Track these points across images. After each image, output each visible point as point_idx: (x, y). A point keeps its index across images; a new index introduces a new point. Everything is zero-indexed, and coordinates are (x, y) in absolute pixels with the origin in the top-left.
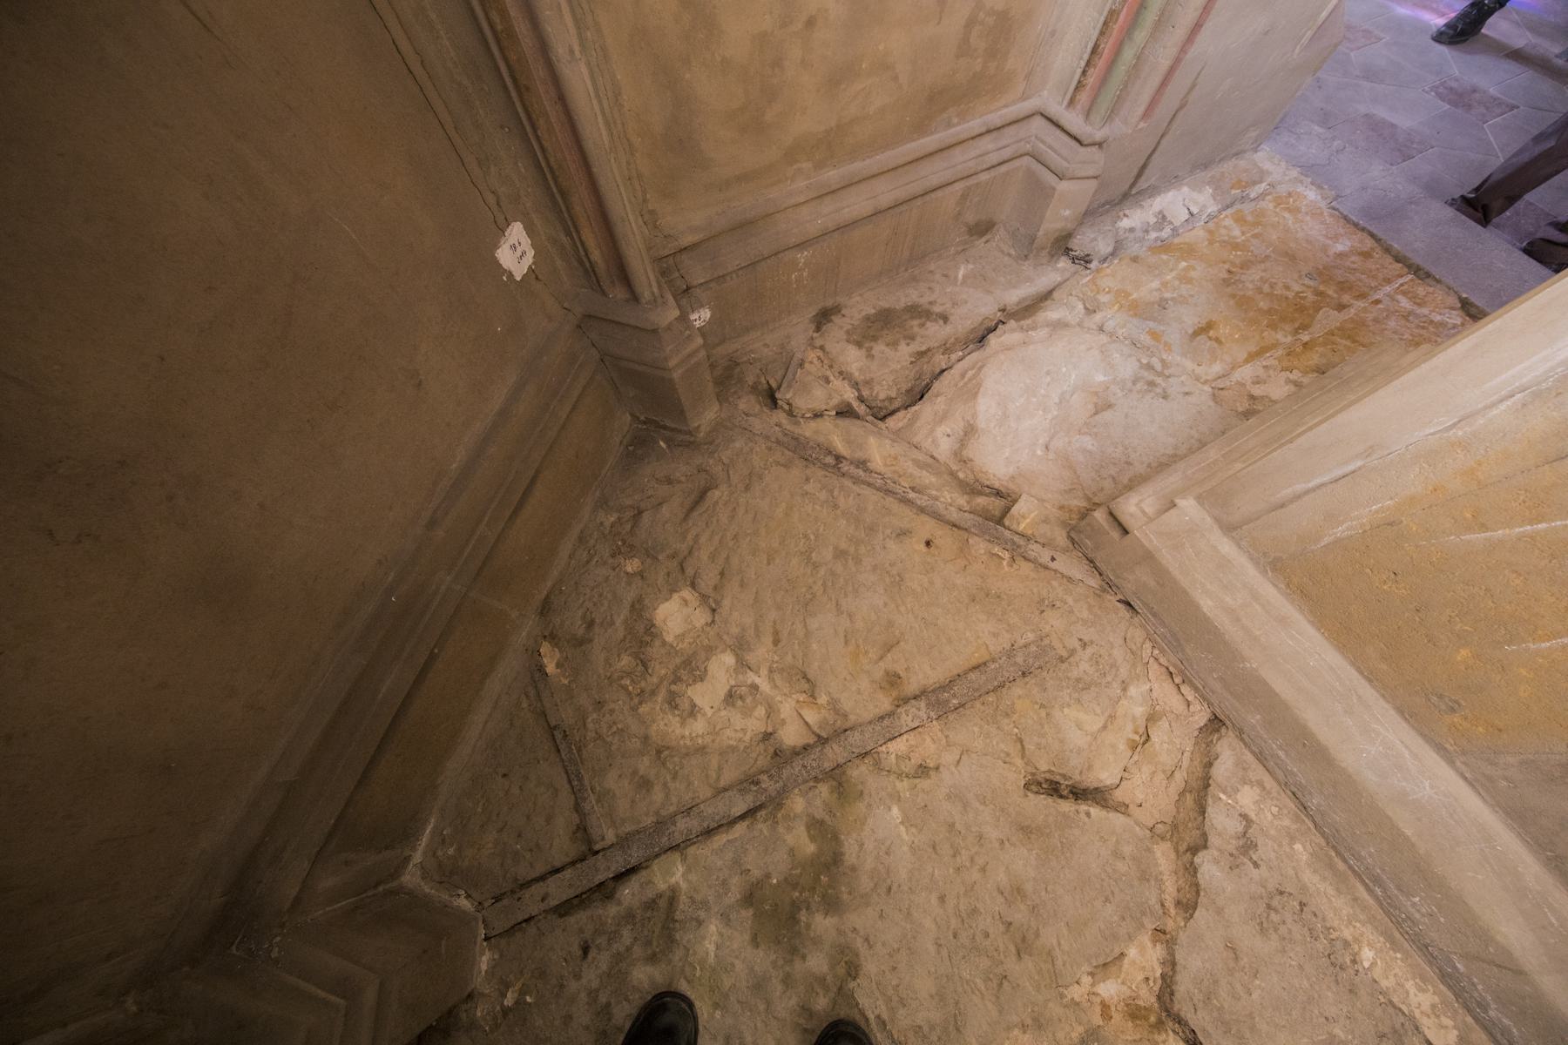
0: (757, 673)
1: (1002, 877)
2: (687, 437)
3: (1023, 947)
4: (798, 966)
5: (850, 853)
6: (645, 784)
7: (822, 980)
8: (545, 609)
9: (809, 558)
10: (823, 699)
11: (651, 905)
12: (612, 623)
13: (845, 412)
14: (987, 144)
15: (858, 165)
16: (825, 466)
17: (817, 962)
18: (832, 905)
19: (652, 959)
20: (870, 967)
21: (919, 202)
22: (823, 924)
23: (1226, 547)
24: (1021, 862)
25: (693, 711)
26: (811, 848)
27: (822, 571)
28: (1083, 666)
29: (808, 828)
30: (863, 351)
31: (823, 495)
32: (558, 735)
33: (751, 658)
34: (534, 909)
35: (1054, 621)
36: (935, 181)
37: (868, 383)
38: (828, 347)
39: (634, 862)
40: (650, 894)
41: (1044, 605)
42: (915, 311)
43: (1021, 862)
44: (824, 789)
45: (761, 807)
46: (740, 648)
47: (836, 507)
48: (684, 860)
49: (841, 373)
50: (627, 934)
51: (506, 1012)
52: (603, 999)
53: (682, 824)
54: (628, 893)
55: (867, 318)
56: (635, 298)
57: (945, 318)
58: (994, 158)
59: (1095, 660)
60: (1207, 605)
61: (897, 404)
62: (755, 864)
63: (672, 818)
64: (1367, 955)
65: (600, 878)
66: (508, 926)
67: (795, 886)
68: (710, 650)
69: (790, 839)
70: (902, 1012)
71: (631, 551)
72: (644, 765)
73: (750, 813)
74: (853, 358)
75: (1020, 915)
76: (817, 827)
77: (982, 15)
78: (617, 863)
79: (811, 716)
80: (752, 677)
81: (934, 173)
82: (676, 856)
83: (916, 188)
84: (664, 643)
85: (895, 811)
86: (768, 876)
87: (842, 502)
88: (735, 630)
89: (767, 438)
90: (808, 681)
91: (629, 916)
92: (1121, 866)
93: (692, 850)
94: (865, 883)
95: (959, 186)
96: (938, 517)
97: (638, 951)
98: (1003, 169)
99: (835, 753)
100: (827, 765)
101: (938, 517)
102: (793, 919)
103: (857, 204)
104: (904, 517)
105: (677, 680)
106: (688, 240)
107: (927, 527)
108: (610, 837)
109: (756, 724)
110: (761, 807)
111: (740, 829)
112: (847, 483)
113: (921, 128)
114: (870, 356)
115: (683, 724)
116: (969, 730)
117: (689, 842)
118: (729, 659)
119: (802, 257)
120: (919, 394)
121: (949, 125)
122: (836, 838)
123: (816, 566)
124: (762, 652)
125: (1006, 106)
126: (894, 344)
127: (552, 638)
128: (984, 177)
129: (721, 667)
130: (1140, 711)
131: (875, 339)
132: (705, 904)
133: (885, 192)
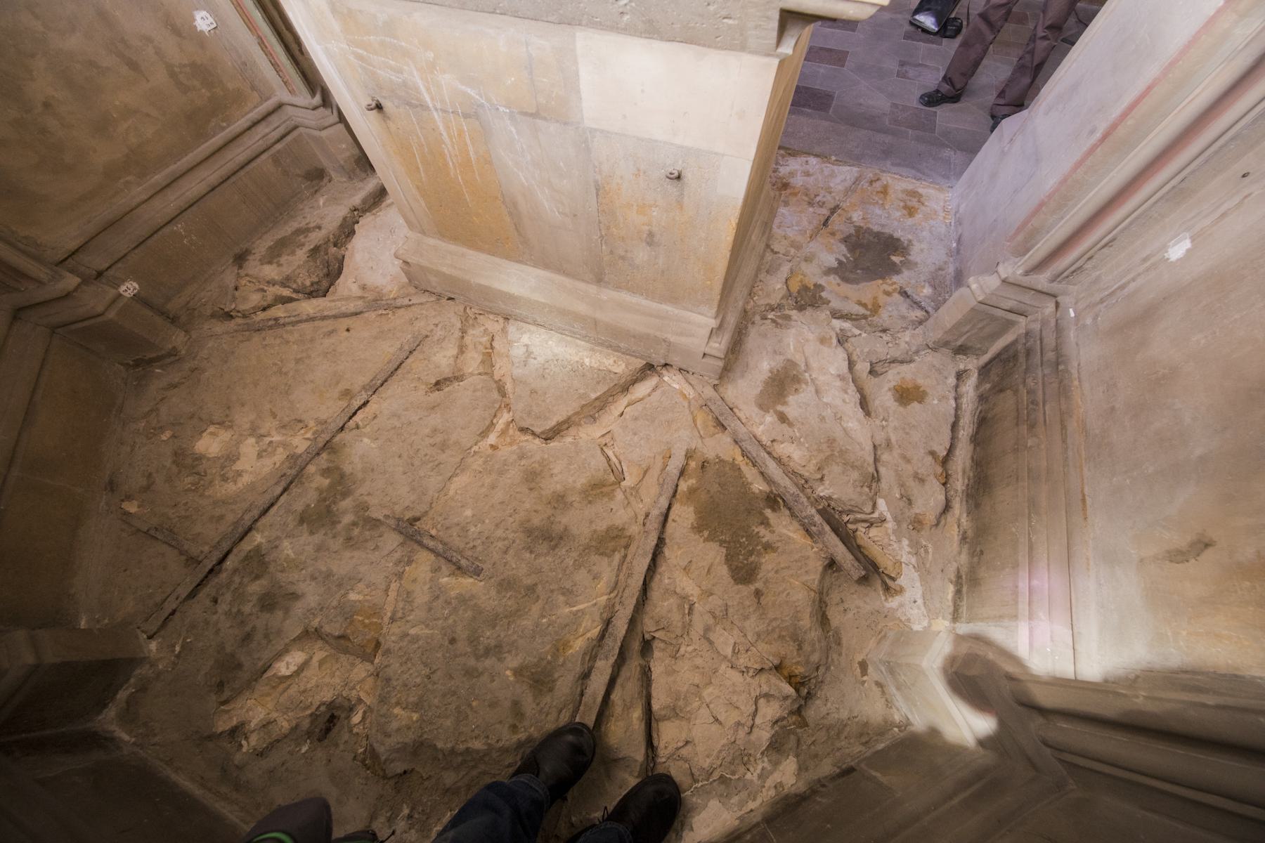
0: (269, 435)
1: (427, 431)
2: (172, 359)
3: (443, 447)
4: (339, 527)
5: (347, 469)
6: (221, 517)
7: (354, 524)
8: (112, 486)
9: (281, 373)
10: (312, 424)
11: (248, 558)
12: (164, 467)
13: (287, 300)
14: (262, 129)
15: (172, 168)
16: (271, 328)
17: (347, 519)
18: (345, 495)
19: (257, 577)
20: (373, 501)
21: (242, 173)
22: (346, 503)
23: (432, 241)
24: (435, 420)
25: (239, 474)
26: (327, 482)
27: (291, 374)
28: (439, 333)
29: (322, 475)
30: (275, 266)
31: (278, 341)
32: (152, 532)
33: (262, 431)
34: (174, 606)
35: (420, 325)
36: (242, 158)
37: (288, 278)
38: (250, 272)
39: (225, 550)
40: (243, 554)
41: (411, 322)
42: (299, 232)
43: (435, 420)
44: (324, 455)
45: (291, 482)
46: (254, 431)
47: (288, 342)
48: (258, 531)
49: (268, 282)
50: (237, 579)
51: (178, 656)
52: (234, 610)
53: (247, 517)
54: (228, 563)
55: (270, 247)
56: (40, 283)
57: (319, 228)
58: (276, 135)
59: (444, 327)
60: (444, 269)
61: (325, 284)
62: (299, 506)
63: (242, 518)
64: (587, 361)
65: (210, 567)
66: (160, 623)
67: (325, 500)
68: (239, 443)
69: (314, 485)
70: (396, 507)
71: (162, 429)
72: (218, 512)
73: (285, 490)
74: (270, 271)
75: (439, 439)
76: (326, 472)
77: (176, 69)
78: (217, 555)
79: (309, 435)
80: (268, 440)
81: (239, 154)
82: (254, 532)
83: (231, 166)
84: (209, 459)
85: (366, 440)
86: (308, 506)
87: (292, 339)
88: (247, 426)
89: (227, 333)
90: (300, 421)
91: (235, 571)
92: (478, 394)
93: (259, 524)
94: (360, 475)
95: (264, 157)
96: (345, 315)
97: (246, 580)
98: (289, 138)
99: (326, 437)
100: (321, 445)
101: (345, 315)
102: (328, 510)
103: (193, 187)
104: (328, 325)
105: (223, 468)
106: (73, 245)
107: (346, 322)
108: (206, 549)
109: (280, 456)
110: (291, 482)
111: (282, 499)
112: (289, 328)
113: (202, 136)
114: (280, 265)
115: (235, 482)
116: (393, 388)
117: (256, 521)
118: (252, 440)
119: (179, 227)
120: (334, 272)
121: (223, 129)
122: (338, 468)
123: (286, 374)
124: (269, 424)
125: (255, 107)
126: (293, 253)
127: (129, 498)
128: (278, 146)
129: (249, 447)
130: (485, 339)
131: (279, 255)
132: (278, 538)
133: (210, 175)
